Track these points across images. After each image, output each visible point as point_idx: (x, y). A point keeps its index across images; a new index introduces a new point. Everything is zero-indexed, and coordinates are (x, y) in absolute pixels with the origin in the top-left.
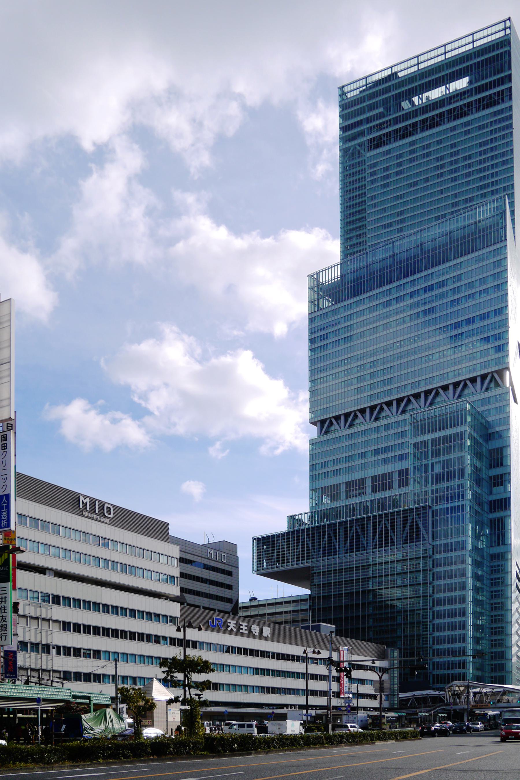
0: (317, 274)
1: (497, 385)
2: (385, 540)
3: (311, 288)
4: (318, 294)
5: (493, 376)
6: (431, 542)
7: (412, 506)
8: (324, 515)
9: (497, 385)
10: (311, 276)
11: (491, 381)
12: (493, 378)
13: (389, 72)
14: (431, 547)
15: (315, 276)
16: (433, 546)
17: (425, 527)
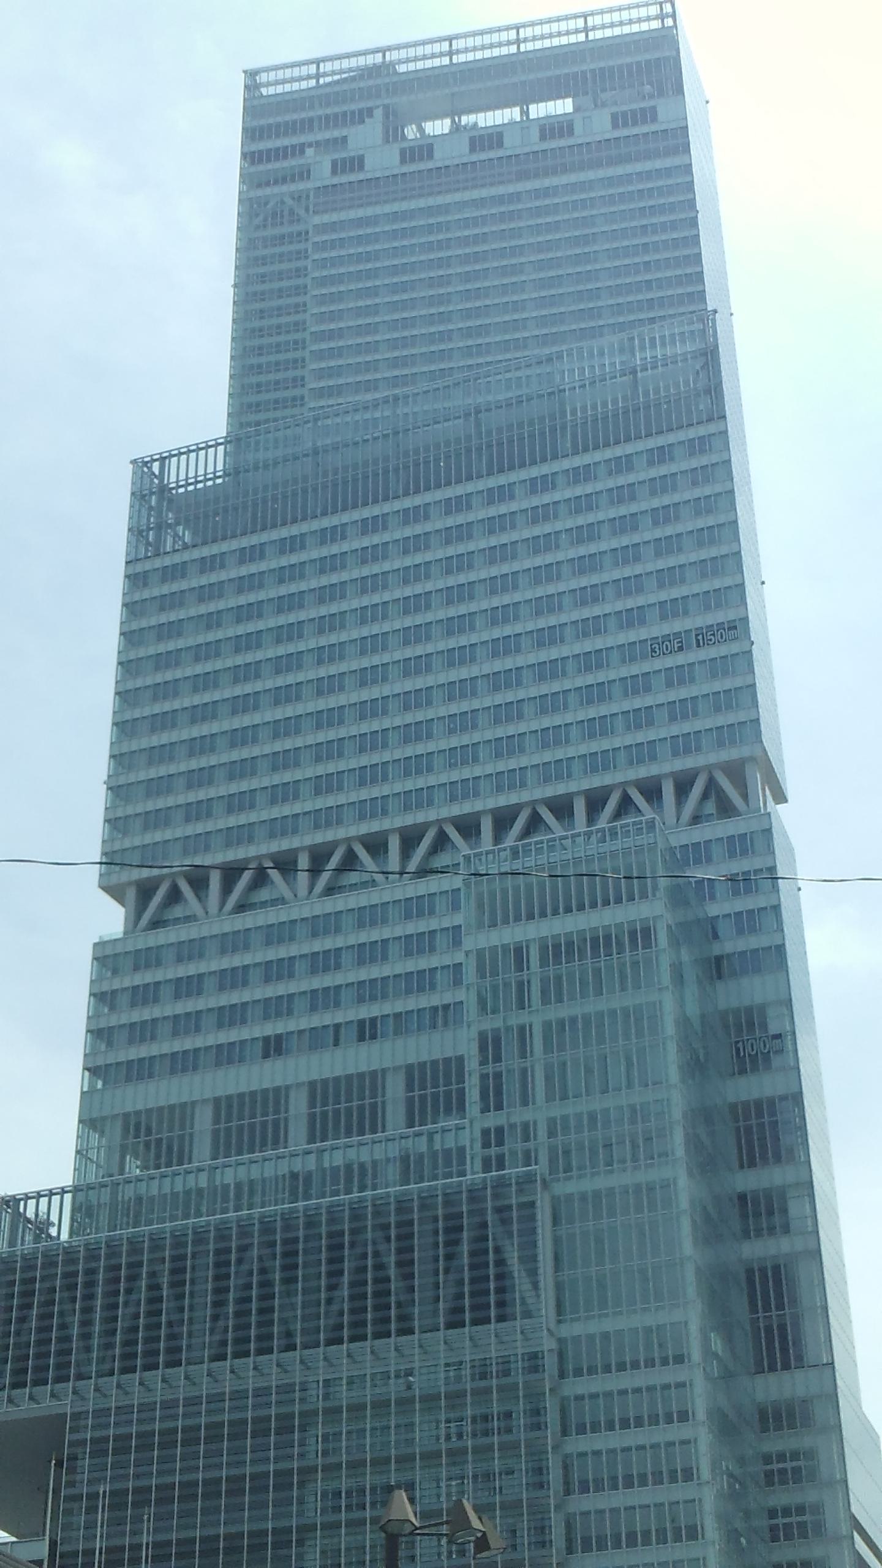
0: (162, 460)
1: (726, 809)
2: (376, 1313)
3: (139, 496)
4: (159, 514)
5: (711, 783)
6: (552, 1326)
7: (475, 1175)
8: (138, 1210)
9: (726, 809)
10: (141, 466)
11: (705, 796)
12: (712, 785)
13: (379, 58)
14: (554, 1345)
15: (156, 467)
16: (561, 1341)
17: (530, 1260)
